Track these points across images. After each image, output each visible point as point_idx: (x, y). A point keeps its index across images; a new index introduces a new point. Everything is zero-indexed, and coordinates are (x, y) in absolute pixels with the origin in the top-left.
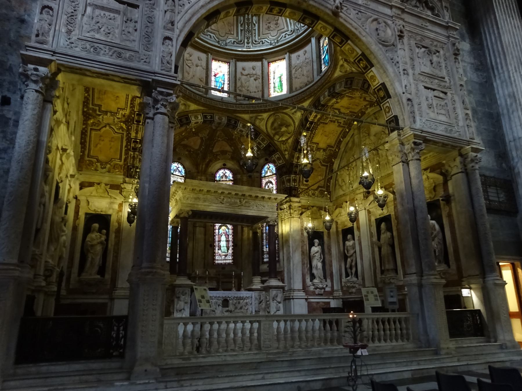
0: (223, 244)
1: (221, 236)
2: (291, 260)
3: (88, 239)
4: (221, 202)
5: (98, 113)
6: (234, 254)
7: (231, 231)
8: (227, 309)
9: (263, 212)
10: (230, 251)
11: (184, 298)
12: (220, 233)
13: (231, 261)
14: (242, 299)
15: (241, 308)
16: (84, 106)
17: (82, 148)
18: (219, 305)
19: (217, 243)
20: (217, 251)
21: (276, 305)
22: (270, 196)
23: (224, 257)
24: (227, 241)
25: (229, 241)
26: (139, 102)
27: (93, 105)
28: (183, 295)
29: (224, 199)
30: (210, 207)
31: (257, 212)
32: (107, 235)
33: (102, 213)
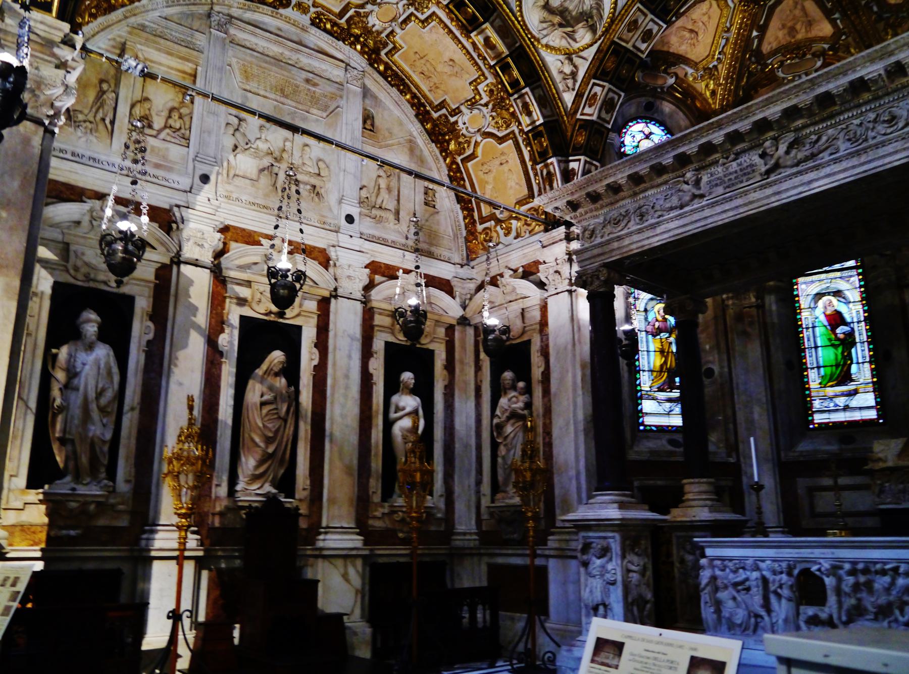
3: (498, 412)
4: (694, 197)
5: (452, 120)
8: (810, 611)
9: (881, 151)
11: (603, 567)
14: (884, 572)
16: (422, 122)
17: (463, 209)
18: (779, 596)
22: (893, 59)
26: (482, 41)
27: (436, 112)
28: (596, 556)
29: (697, 183)
30: (659, 230)
31: (855, 161)
32: (528, 391)
33: (514, 342)
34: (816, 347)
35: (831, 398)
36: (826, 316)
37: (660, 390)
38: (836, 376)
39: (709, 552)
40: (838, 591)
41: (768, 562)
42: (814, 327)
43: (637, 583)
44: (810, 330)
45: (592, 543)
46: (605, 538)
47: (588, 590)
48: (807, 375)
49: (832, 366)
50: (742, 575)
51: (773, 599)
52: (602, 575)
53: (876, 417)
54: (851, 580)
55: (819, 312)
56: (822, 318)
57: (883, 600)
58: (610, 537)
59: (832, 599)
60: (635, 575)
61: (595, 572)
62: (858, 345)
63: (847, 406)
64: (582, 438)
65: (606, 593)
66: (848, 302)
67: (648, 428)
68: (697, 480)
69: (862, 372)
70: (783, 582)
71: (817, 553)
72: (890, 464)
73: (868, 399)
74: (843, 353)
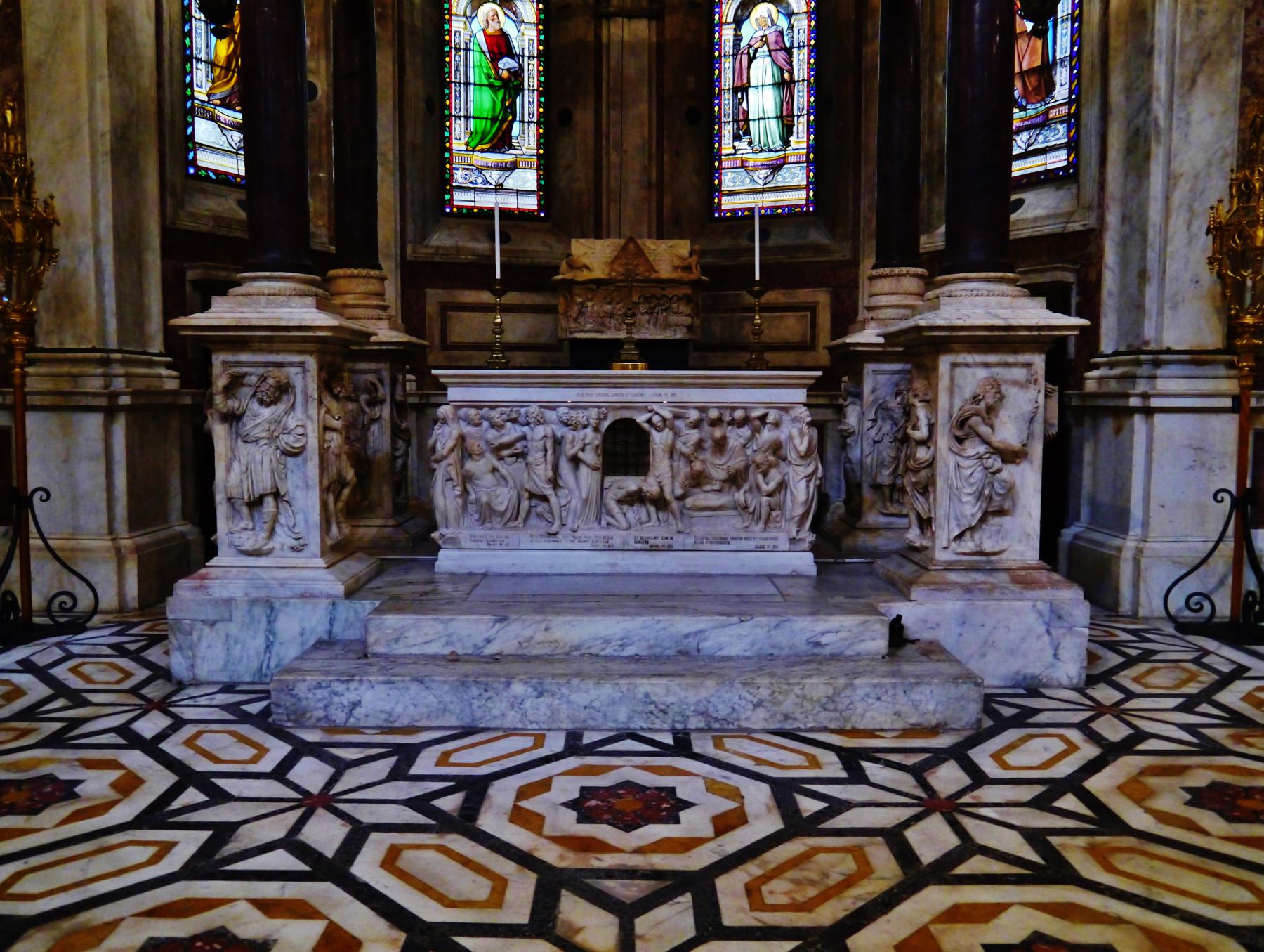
0: (763, 101)
1: (751, 60)
2: (1158, 153)
6: (819, 158)
7: (802, 24)
10: (800, 141)
12: (744, 44)
13: (803, 194)
14: (746, 421)
15: (735, 480)
18: (576, 461)
19: (727, 100)
20: (727, 144)
21: (978, 475)
23: (763, 173)
24: (784, 85)
25: (792, 81)
34: (467, 84)
35: (480, 170)
36: (486, 35)
37: (225, 104)
38: (490, 136)
39: (454, 394)
40: (672, 451)
41: (562, 411)
42: (467, 50)
43: (336, 451)
44: (462, 53)
45: (246, 374)
46: (280, 365)
47: (236, 465)
48: (450, 127)
49: (486, 119)
50: (512, 432)
51: (565, 467)
52: (272, 439)
53: (536, 207)
54: (694, 435)
55: (477, 26)
56: (481, 38)
57: (737, 463)
58: (292, 364)
59: (661, 465)
60: (334, 436)
61: (257, 433)
62: (526, 92)
63: (501, 185)
64: (106, 167)
65: (279, 473)
66: (519, 22)
67: (203, 173)
68: (364, 272)
69: (526, 138)
70: (587, 441)
71: (649, 394)
72: (599, 273)
73: (528, 179)
74: (503, 101)
